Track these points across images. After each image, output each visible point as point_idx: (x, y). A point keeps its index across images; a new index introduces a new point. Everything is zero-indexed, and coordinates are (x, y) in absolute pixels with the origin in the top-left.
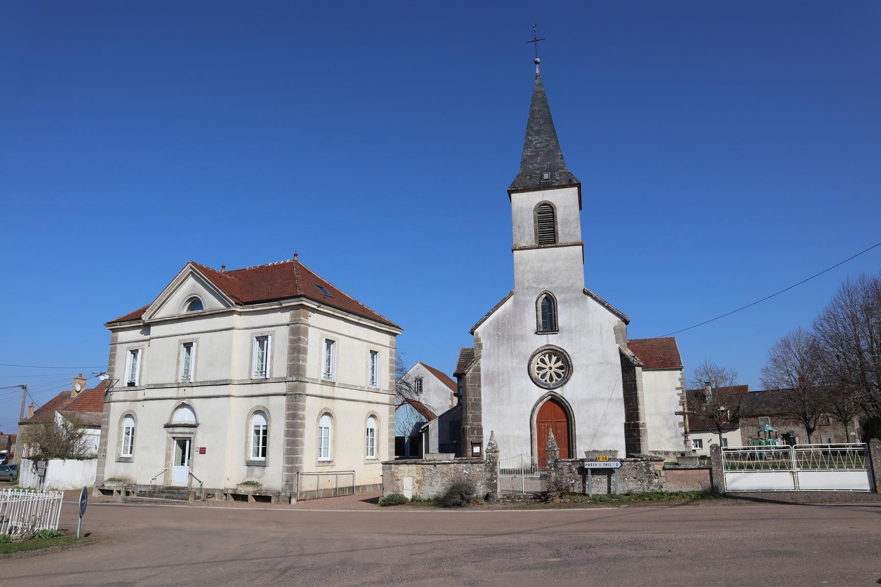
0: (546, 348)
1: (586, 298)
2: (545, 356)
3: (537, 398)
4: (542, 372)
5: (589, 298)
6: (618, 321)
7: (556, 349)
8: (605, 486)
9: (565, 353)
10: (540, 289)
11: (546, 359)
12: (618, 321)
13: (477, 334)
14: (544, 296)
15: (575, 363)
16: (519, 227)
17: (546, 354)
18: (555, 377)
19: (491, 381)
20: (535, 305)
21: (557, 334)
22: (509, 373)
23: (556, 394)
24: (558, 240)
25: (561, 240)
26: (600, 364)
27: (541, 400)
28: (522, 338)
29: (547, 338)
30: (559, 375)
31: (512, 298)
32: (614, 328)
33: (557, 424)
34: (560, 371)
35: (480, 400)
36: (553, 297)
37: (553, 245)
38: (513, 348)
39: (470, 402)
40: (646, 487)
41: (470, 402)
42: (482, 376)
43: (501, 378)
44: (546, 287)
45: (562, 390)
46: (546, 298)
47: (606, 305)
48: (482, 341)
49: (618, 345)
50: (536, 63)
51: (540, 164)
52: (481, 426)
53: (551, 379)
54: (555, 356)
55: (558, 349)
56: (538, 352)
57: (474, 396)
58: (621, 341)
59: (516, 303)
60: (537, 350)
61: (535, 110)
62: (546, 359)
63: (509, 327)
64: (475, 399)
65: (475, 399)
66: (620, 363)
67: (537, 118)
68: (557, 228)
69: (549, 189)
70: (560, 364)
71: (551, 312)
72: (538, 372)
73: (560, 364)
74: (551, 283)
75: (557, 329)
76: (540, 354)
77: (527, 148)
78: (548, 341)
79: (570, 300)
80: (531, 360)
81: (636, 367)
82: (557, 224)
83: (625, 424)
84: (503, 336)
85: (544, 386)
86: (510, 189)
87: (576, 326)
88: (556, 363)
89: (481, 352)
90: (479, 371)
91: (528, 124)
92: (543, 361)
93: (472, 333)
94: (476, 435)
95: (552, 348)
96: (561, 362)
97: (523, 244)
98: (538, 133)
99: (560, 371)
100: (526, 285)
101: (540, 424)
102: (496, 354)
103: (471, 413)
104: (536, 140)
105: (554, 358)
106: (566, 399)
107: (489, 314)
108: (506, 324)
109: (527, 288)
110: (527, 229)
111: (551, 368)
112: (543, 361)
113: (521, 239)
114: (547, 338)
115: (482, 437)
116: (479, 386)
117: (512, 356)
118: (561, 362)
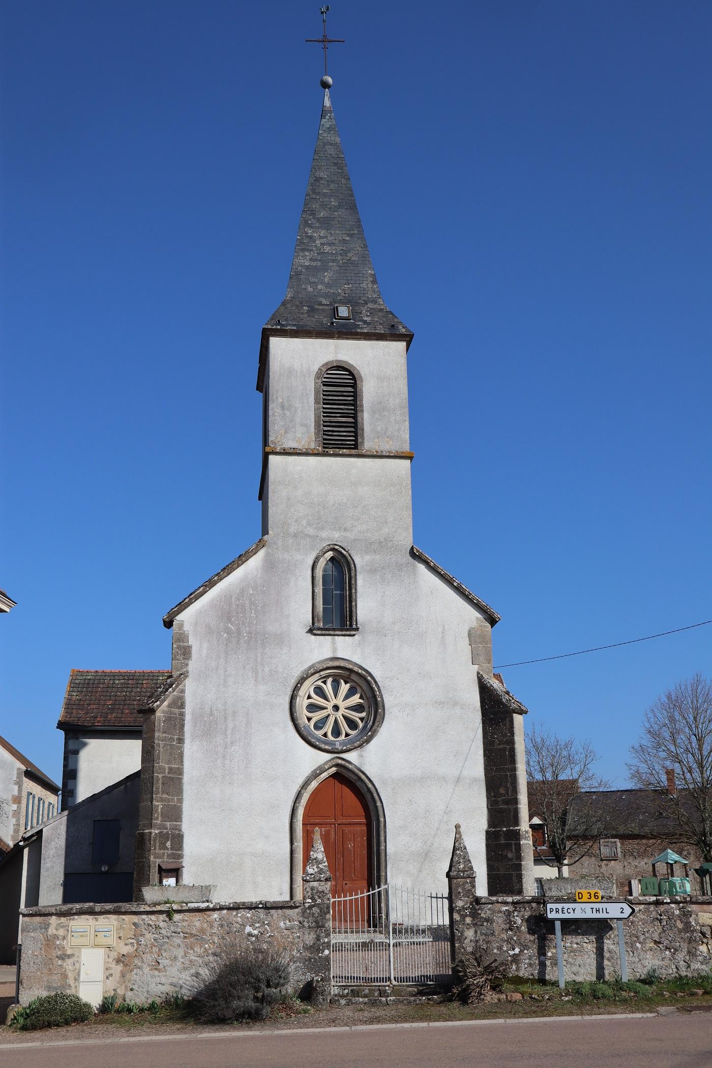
0: (331, 664)
1: (414, 566)
2: (325, 682)
3: (307, 771)
4: (317, 716)
5: (421, 567)
6: (477, 619)
7: (350, 667)
8: (590, 960)
9: (369, 678)
10: (322, 540)
11: (328, 688)
12: (477, 619)
13: (181, 625)
14: (330, 554)
15: (389, 700)
16: (283, 407)
17: (328, 677)
18: (344, 727)
19: (208, 730)
20: (310, 572)
21: (353, 635)
22: (247, 714)
23: (347, 765)
24: (363, 443)
25: (369, 443)
26: (440, 704)
27: (315, 775)
28: (280, 639)
29: (334, 643)
30: (352, 724)
31: (261, 553)
32: (470, 631)
33: (346, 829)
34: (355, 716)
35: (180, 772)
36: (349, 558)
37: (353, 452)
38: (259, 660)
39: (160, 776)
40: (682, 963)
41: (160, 776)
42: (188, 718)
43: (230, 725)
44: (336, 536)
45: (361, 756)
46: (332, 559)
47: (455, 584)
48: (192, 641)
49: (476, 667)
50: (325, 85)
51: (328, 285)
52: (180, 830)
53: (336, 732)
54: (346, 683)
55: (356, 669)
56: (312, 671)
57: (169, 762)
58: (482, 658)
59: (270, 565)
60: (310, 668)
61: (321, 178)
62: (328, 688)
63: (253, 615)
64: (170, 769)
65: (170, 769)
66: (479, 704)
67: (325, 195)
68: (362, 419)
69: (348, 339)
70: (356, 699)
71: (342, 589)
72: (310, 715)
73: (356, 699)
74: (345, 530)
75: (354, 626)
76: (316, 676)
77: (303, 250)
78: (334, 650)
79: (383, 568)
80: (296, 689)
81: (514, 715)
82: (362, 411)
83: (487, 832)
84: (239, 632)
85: (323, 746)
86: (270, 327)
87: (393, 623)
88: (347, 697)
89: (187, 665)
90: (182, 706)
91: (306, 204)
92: (320, 691)
93: (169, 624)
94: (170, 852)
95: (342, 664)
96: (358, 696)
97: (290, 444)
98: (326, 223)
99: (355, 716)
100: (292, 530)
101: (309, 827)
102: (222, 671)
103: (162, 800)
104: (321, 238)
105: (344, 688)
106: (368, 775)
107: (210, 584)
108: (247, 607)
109: (295, 535)
110: (299, 412)
111: (336, 708)
112: (320, 691)
113: (286, 432)
114: (334, 643)
115: (180, 856)
116: (181, 741)
117: (256, 677)
118: (358, 696)
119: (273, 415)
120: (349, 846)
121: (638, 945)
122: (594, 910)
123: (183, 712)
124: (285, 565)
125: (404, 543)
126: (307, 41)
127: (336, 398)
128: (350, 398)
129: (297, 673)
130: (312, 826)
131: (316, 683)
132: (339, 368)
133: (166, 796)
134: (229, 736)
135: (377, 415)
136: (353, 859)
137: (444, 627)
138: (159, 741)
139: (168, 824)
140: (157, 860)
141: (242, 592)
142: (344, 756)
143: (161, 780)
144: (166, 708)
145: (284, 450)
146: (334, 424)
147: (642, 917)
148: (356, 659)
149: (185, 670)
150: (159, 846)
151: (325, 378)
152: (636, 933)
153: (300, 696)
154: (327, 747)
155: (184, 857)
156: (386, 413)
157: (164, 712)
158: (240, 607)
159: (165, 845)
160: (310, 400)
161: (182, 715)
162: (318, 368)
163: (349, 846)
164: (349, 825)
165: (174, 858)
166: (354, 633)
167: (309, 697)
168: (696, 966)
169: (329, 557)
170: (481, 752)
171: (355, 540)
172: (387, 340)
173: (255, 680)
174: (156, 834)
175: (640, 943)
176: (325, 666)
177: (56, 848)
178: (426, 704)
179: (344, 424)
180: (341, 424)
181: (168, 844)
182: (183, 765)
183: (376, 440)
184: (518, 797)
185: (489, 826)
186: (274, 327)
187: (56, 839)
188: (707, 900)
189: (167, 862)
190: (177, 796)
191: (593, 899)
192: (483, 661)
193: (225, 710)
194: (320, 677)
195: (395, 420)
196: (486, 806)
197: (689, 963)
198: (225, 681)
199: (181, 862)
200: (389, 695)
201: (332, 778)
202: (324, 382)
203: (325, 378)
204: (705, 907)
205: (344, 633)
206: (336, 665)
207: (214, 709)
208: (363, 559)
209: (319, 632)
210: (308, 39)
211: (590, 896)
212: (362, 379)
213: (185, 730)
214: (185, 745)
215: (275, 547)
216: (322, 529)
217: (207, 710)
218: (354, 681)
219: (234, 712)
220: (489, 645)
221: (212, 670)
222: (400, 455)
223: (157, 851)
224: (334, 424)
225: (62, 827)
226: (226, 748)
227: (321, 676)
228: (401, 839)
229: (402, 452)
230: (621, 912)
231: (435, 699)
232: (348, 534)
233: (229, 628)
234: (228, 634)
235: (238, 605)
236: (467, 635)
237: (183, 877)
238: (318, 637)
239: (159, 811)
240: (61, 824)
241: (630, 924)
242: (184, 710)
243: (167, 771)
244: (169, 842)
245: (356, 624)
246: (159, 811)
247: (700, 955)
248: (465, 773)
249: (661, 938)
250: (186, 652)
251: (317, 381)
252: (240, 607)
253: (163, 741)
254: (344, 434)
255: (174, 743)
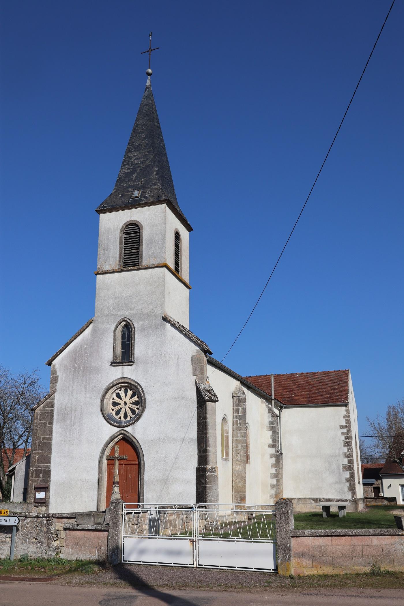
0: (121, 381)
1: (164, 325)
2: (121, 390)
3: (107, 437)
4: (117, 408)
5: (168, 325)
6: (197, 350)
7: (130, 381)
8: (7, 547)
9: (139, 387)
10: (120, 316)
11: (122, 393)
12: (197, 350)
13: (54, 366)
14: (124, 323)
15: (148, 398)
16: (104, 249)
17: (121, 387)
18: (129, 413)
19: (64, 418)
20: (112, 334)
21: (132, 365)
22: (81, 409)
23: (126, 433)
24: (142, 262)
25: (145, 262)
26: (175, 399)
27: (112, 439)
28: (98, 370)
29: (123, 370)
30: (133, 412)
31: (91, 326)
32: (192, 357)
33: (128, 467)
34: (135, 407)
35: (50, 439)
36: (131, 324)
37: (136, 268)
38: (87, 381)
39: (37, 442)
40: (44, 551)
41: (37, 442)
42: (55, 412)
43: (74, 415)
44: (125, 313)
45: (133, 429)
46: (126, 325)
47: (184, 332)
48: (59, 374)
49: (195, 377)
50: (148, 74)
51: (134, 181)
52: (50, 468)
53: (126, 416)
54: (131, 390)
55: (132, 383)
56: (111, 385)
57: (43, 434)
58: (198, 372)
59: (94, 332)
60: (111, 383)
61: (139, 125)
62: (122, 393)
63: (86, 358)
64: (44, 438)
65: (44, 438)
66: (195, 398)
67: (140, 133)
68: (142, 249)
69: (136, 208)
70: (135, 398)
71: (129, 341)
72: (113, 408)
73: (135, 398)
74: (131, 309)
75: (132, 360)
76: (114, 388)
77: (125, 165)
78: (123, 373)
79: (148, 328)
80: (105, 395)
81: (207, 403)
82: (142, 245)
83: (197, 468)
84: (79, 368)
85: (115, 424)
86: (98, 209)
87: (152, 357)
88: (132, 397)
89: (56, 386)
90: (53, 406)
91: (130, 140)
92: (118, 396)
94: (42, 479)
95: (126, 380)
96: (136, 396)
97: (107, 268)
98: (138, 148)
99: (135, 407)
100: (106, 313)
101: (111, 467)
102: (71, 388)
103: (38, 453)
104: (135, 156)
105: (130, 393)
106: (137, 439)
107: (67, 345)
108: (83, 354)
109: (107, 315)
110: (112, 251)
111: (125, 403)
112: (118, 396)
113: (105, 262)
114: (123, 370)
115: (49, 481)
116: (51, 424)
117: (86, 389)
118: (136, 396)
119: (100, 254)
120: (130, 476)
121: (27, 540)
122: (5, 520)
123: (53, 409)
124: (101, 331)
125: (160, 313)
126: (142, 53)
127: (131, 240)
128: (137, 239)
129: (105, 386)
130: (112, 465)
131: (116, 391)
132: (129, 225)
133: (41, 451)
134: (73, 421)
135: (149, 246)
136: (131, 483)
137: (178, 356)
138: (37, 424)
139: (42, 465)
140: (34, 483)
141: (81, 347)
142: (125, 429)
143: (38, 444)
144: (41, 408)
145: (103, 272)
146: (129, 254)
147: (31, 524)
148: (133, 378)
149: (55, 388)
150: (35, 476)
151: (125, 231)
152: (27, 533)
153: (106, 398)
154: (117, 425)
155: (51, 482)
156: (154, 244)
157: (40, 410)
158: (80, 355)
159: (39, 476)
160: (117, 244)
161: (53, 411)
162: (122, 226)
163: (130, 476)
164: (130, 465)
165: (45, 482)
166: (132, 363)
167: (113, 399)
168: (49, 553)
169: (123, 325)
170: (196, 424)
171: (135, 314)
172: (156, 205)
173: (86, 392)
174: (33, 470)
175: (28, 539)
176: (117, 382)
177: (20, 476)
178: (168, 399)
179: (134, 254)
180: (131, 254)
181: (41, 475)
182: (52, 436)
183: (148, 260)
184: (208, 449)
185: (198, 465)
186: (100, 209)
187: (21, 471)
188: (60, 516)
189: (40, 484)
190: (48, 451)
191: (5, 515)
192: (199, 373)
193: (71, 407)
194: (117, 388)
195: (158, 247)
196: (197, 454)
197: (47, 551)
198: (72, 393)
199: (49, 484)
200: (148, 396)
201: (123, 440)
202: (125, 233)
203: (125, 231)
204: (60, 520)
205: (127, 364)
206: (123, 381)
207: (67, 407)
208: (138, 324)
209: (115, 365)
210: (142, 52)
211: (5, 512)
212: (143, 228)
213: (54, 418)
214: (54, 425)
215: (97, 322)
216: (120, 310)
217: (64, 408)
218: (134, 389)
219: (75, 408)
220: (202, 364)
221: (67, 387)
222: (159, 265)
223: (34, 479)
224: (129, 254)
225: (23, 466)
226: (71, 427)
227: (117, 387)
228: (152, 472)
229: (160, 264)
230: (15, 522)
231: (172, 396)
232: (132, 312)
233: (75, 366)
234: (74, 369)
235: (79, 354)
236: (190, 359)
237: (50, 491)
238: (115, 367)
239: (36, 459)
240: (23, 464)
241: (26, 528)
242: (54, 408)
243: (42, 439)
244: (41, 474)
245: (134, 359)
246: (36, 459)
247: (52, 547)
248: (187, 436)
249: (37, 536)
250: (55, 379)
251: (121, 233)
252: (80, 355)
253: (39, 424)
254: (134, 258)
255: (47, 425)
